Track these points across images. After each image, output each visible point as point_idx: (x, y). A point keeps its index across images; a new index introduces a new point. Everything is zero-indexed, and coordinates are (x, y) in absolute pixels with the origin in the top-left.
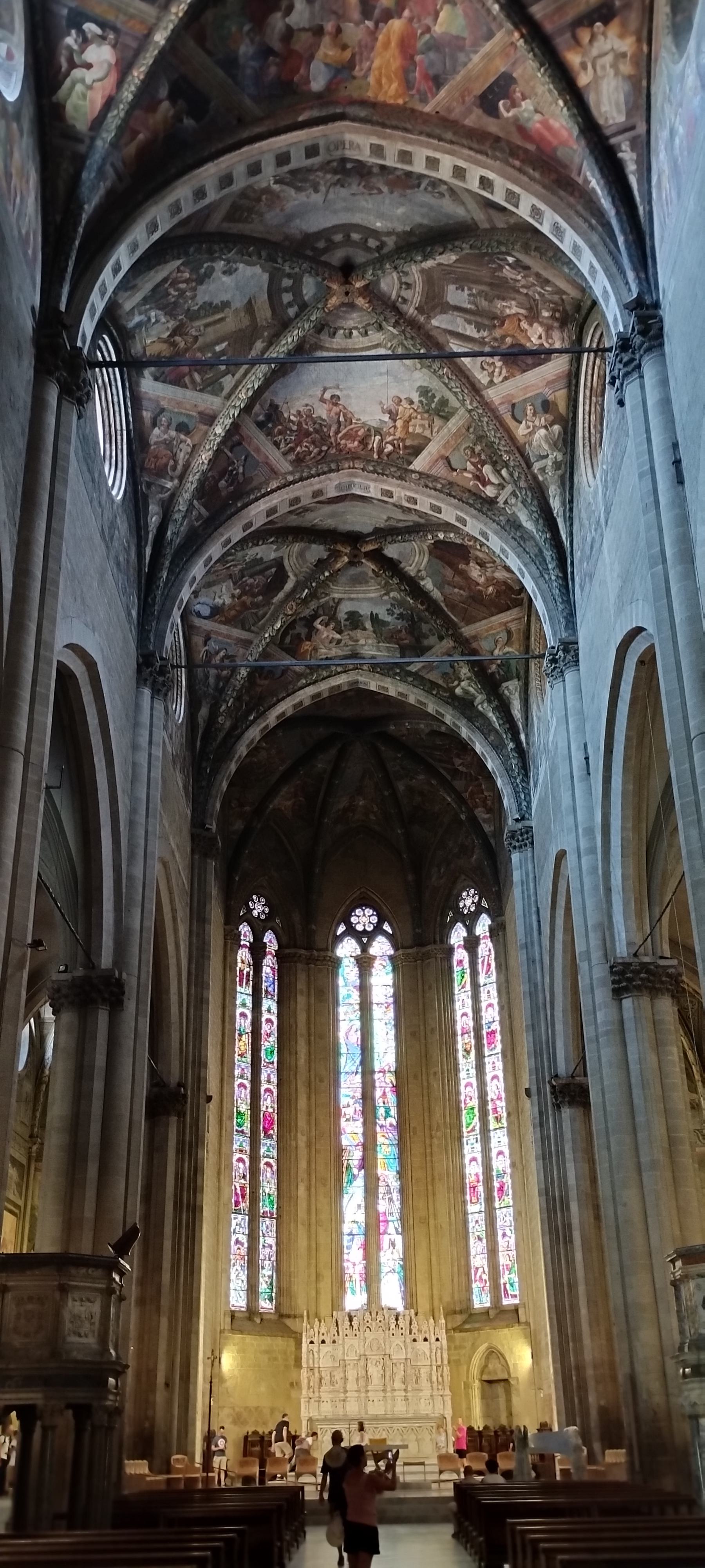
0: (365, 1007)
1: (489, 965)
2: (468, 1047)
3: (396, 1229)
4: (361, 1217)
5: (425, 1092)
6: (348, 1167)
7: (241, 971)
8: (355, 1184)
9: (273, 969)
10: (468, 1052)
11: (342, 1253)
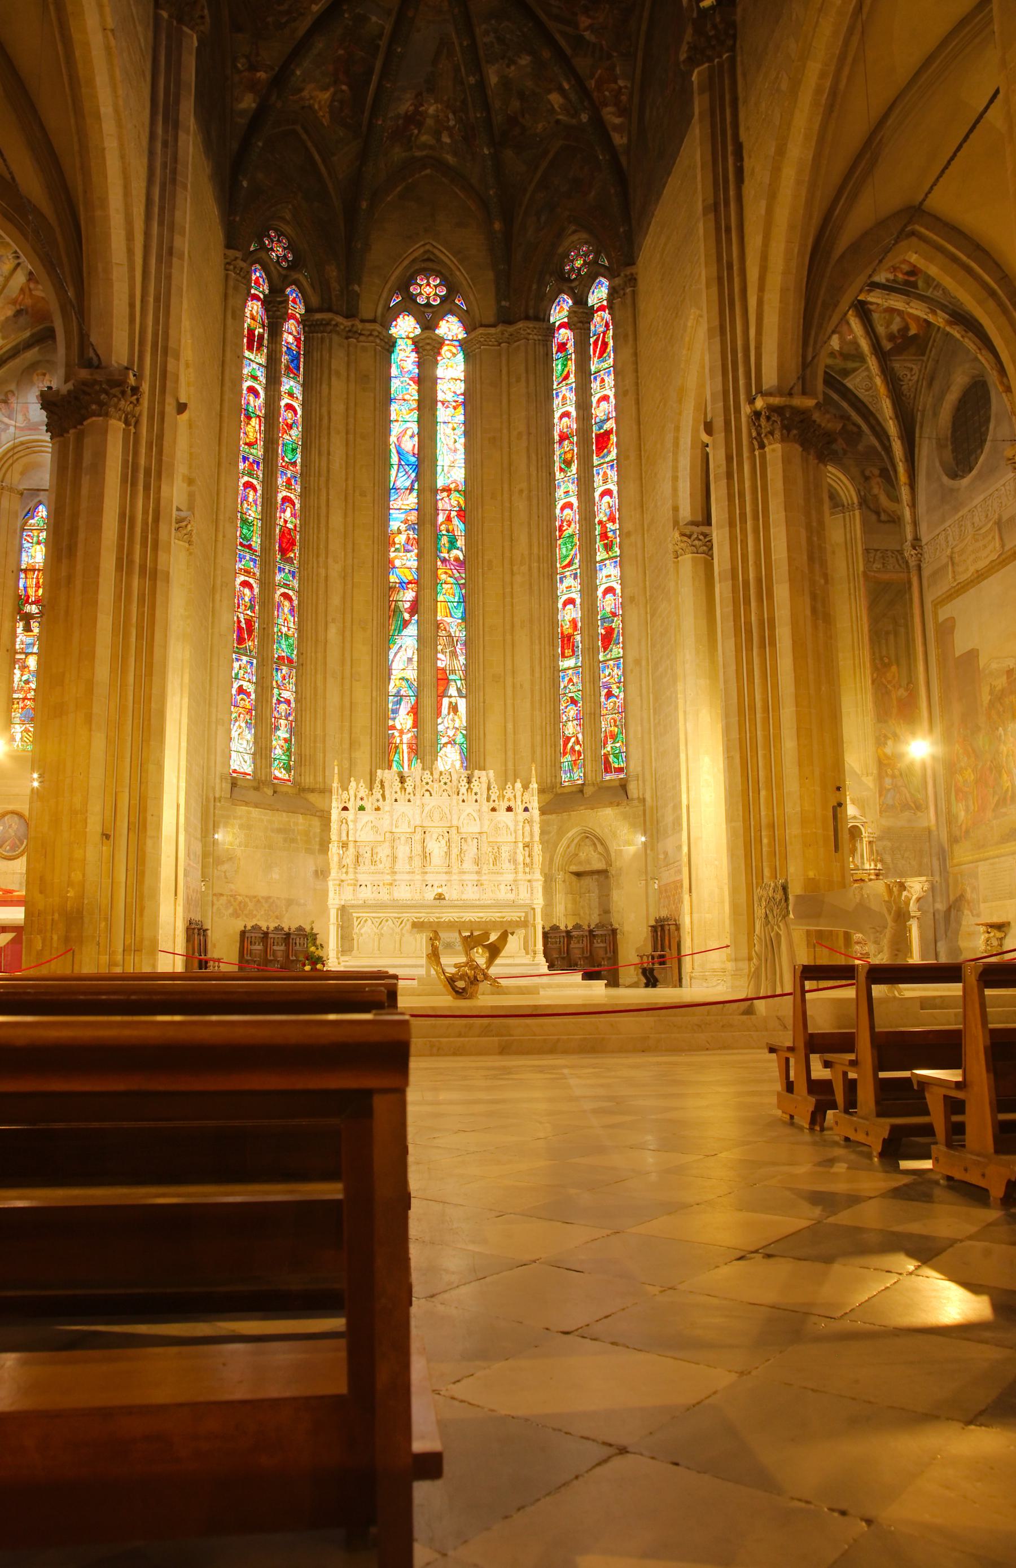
0: (427, 405)
1: (605, 345)
2: (569, 456)
3: (459, 690)
4: (412, 674)
5: (507, 514)
6: (397, 611)
7: (251, 332)
8: (405, 632)
9: (297, 339)
10: (568, 463)
11: (386, 718)
